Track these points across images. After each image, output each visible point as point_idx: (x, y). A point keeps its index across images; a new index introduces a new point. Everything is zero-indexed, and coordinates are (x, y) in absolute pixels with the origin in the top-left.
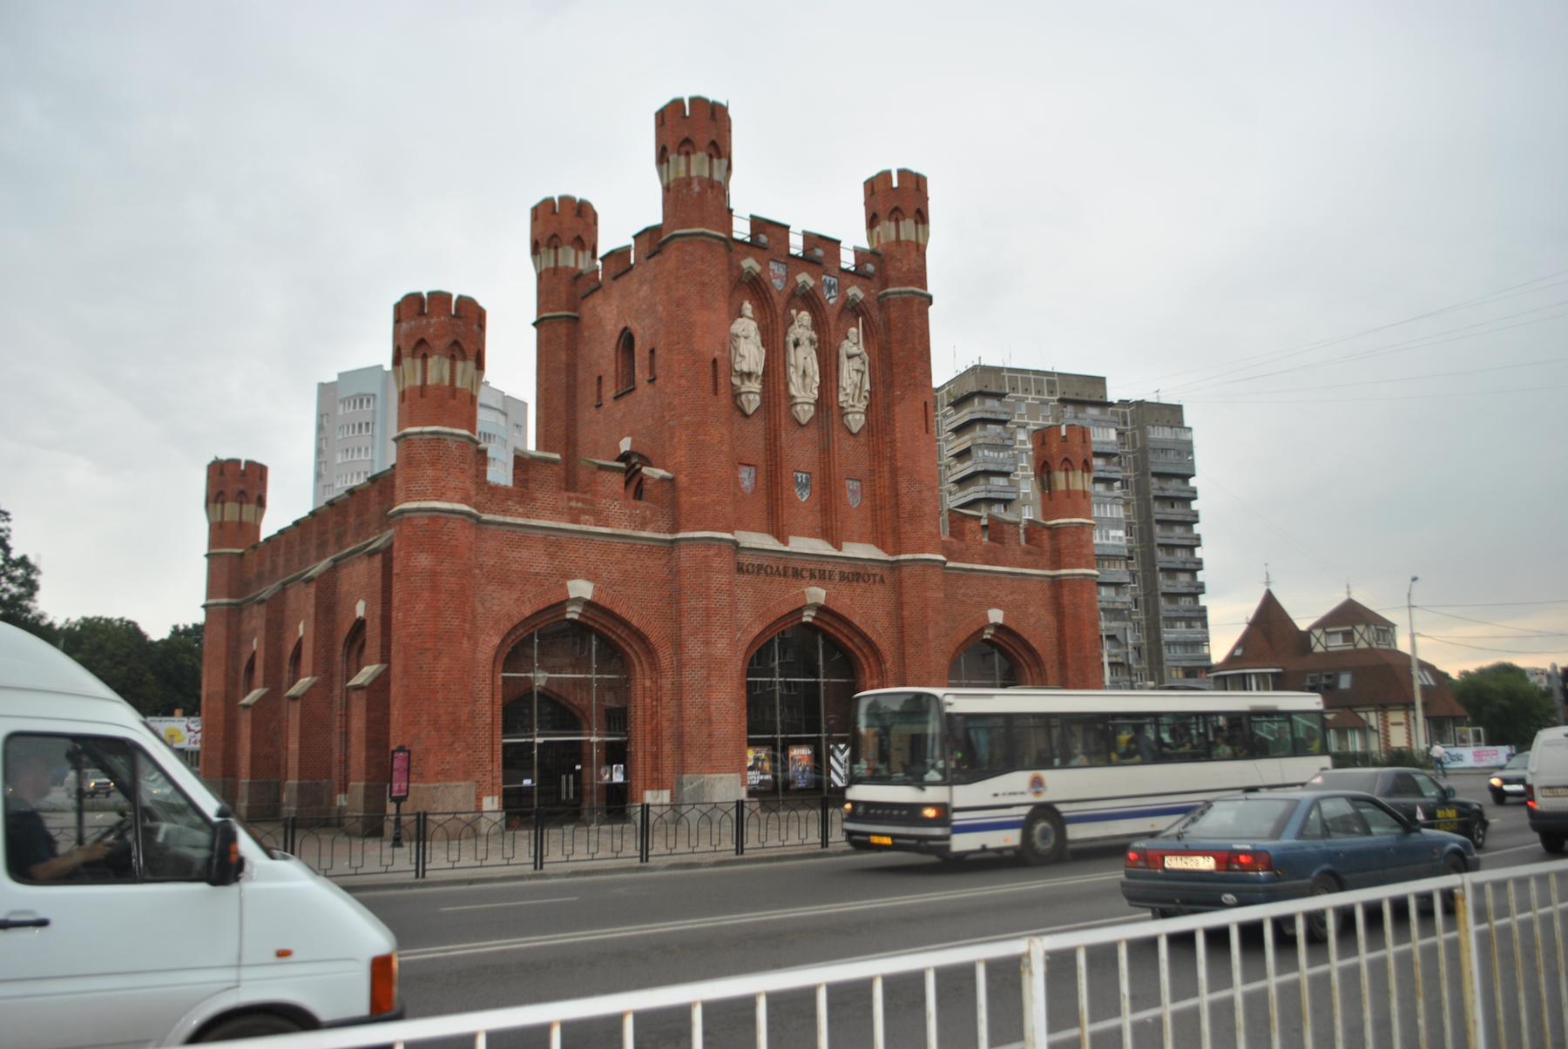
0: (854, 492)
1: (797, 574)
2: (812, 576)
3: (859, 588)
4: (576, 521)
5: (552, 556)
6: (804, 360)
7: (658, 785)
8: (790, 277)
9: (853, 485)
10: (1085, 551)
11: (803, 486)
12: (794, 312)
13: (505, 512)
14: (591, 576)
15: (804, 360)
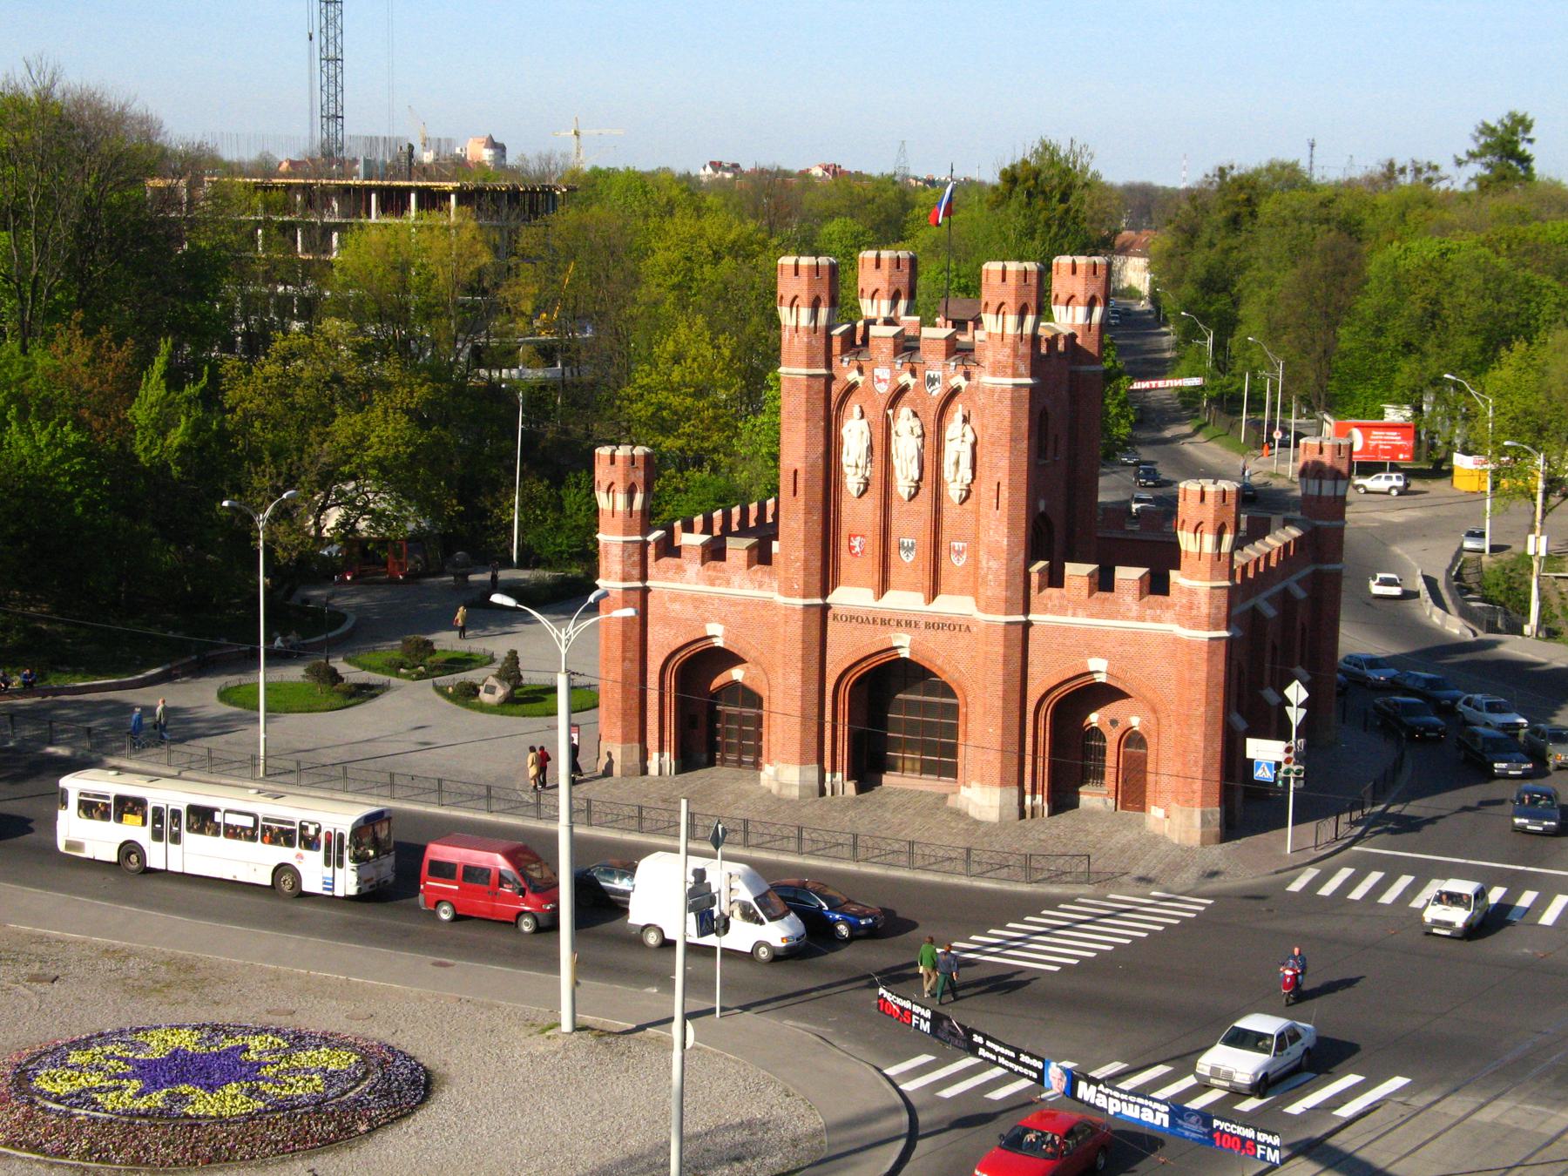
0: (959, 553)
1: (883, 622)
2: (899, 623)
3: (942, 635)
4: (713, 585)
5: (696, 608)
6: (906, 447)
7: (769, 762)
8: (894, 377)
9: (958, 545)
10: (1194, 612)
11: (909, 549)
12: (890, 412)
13: (667, 579)
14: (723, 620)
15: (906, 447)
